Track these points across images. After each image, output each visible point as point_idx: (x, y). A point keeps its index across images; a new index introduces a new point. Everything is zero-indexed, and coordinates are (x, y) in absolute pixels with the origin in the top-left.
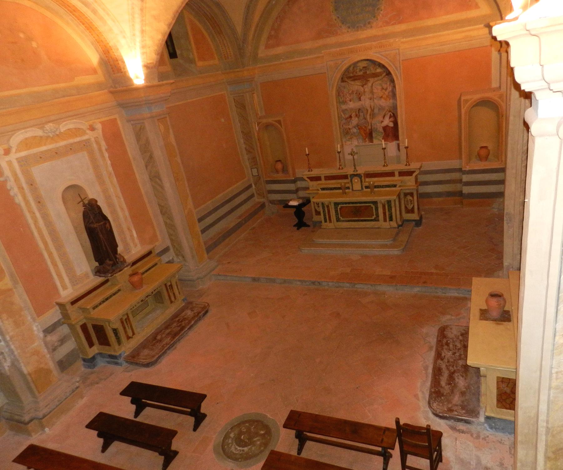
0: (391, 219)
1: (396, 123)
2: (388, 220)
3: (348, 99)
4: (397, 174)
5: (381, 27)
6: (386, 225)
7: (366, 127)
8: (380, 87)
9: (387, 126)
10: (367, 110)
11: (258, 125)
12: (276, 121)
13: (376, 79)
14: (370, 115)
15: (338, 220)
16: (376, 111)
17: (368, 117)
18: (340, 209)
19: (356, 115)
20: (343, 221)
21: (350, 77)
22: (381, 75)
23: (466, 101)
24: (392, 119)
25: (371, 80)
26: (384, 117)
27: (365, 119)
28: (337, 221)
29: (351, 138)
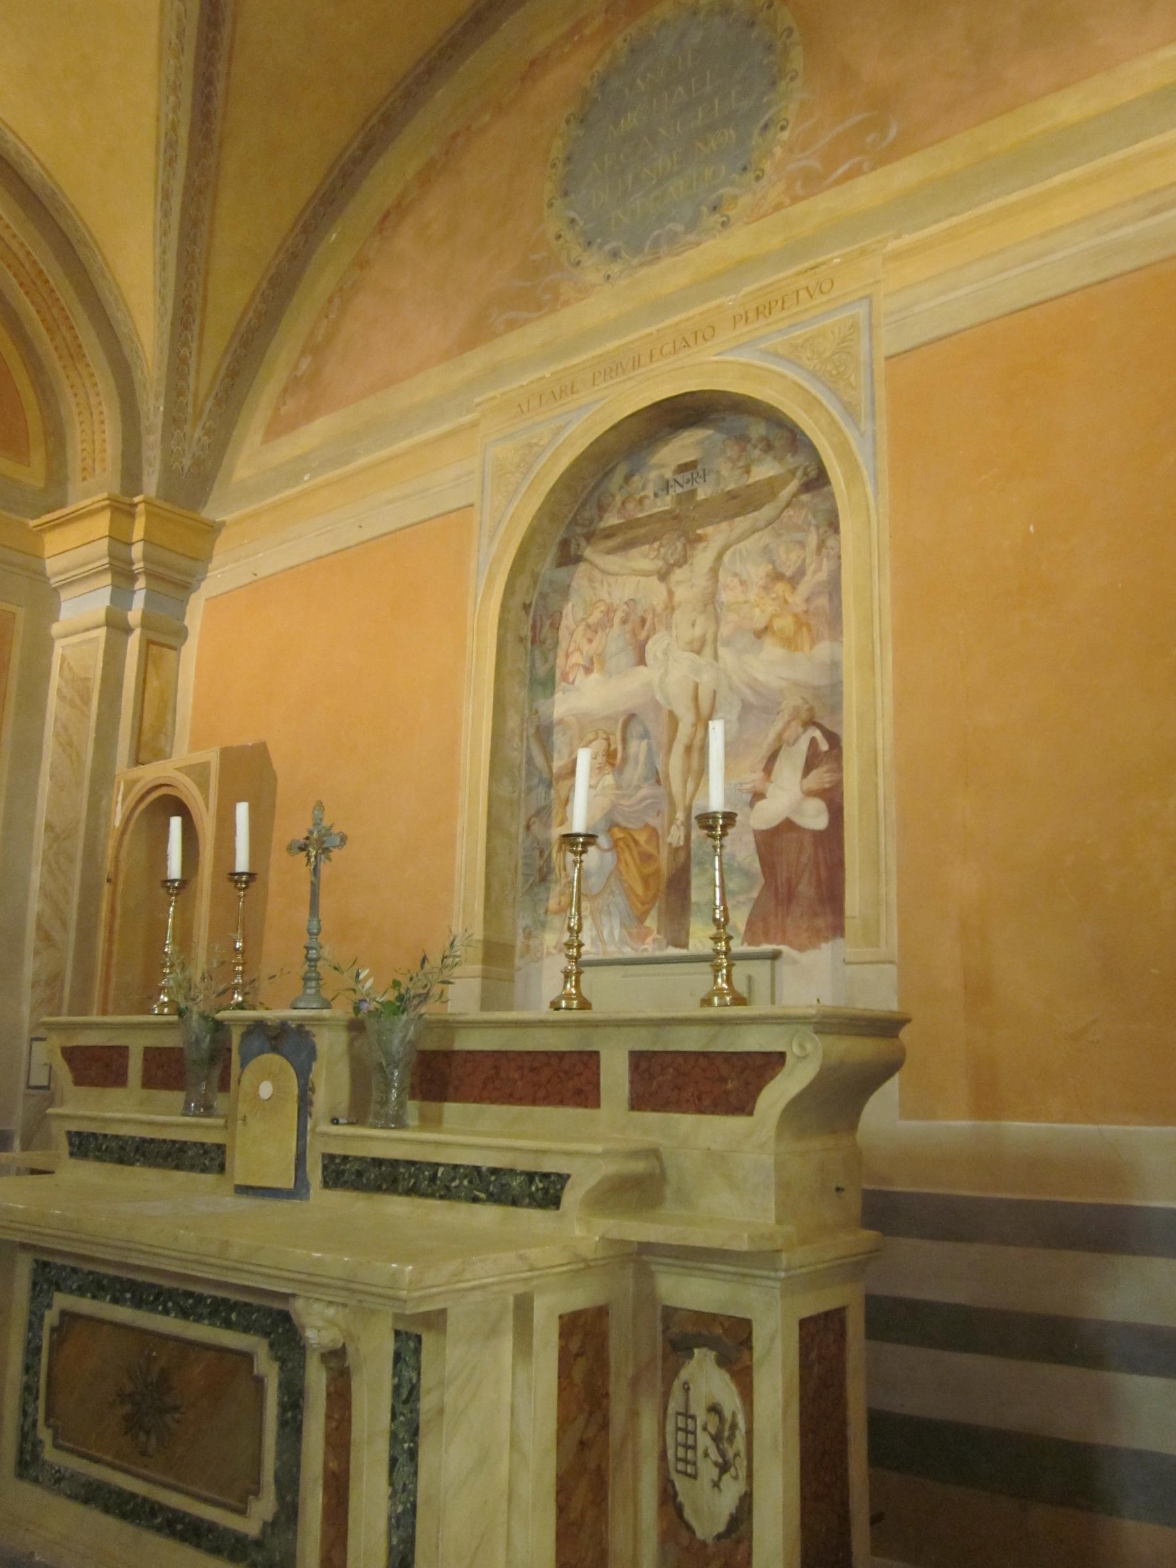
3: (576, 658)
4: (615, 1074)
5: (778, 207)
7: (654, 834)
9: (788, 826)
13: (742, 523)
20: (57, 1481)
22: (774, 495)
25: (717, 534)
26: (772, 758)
27: (657, 778)
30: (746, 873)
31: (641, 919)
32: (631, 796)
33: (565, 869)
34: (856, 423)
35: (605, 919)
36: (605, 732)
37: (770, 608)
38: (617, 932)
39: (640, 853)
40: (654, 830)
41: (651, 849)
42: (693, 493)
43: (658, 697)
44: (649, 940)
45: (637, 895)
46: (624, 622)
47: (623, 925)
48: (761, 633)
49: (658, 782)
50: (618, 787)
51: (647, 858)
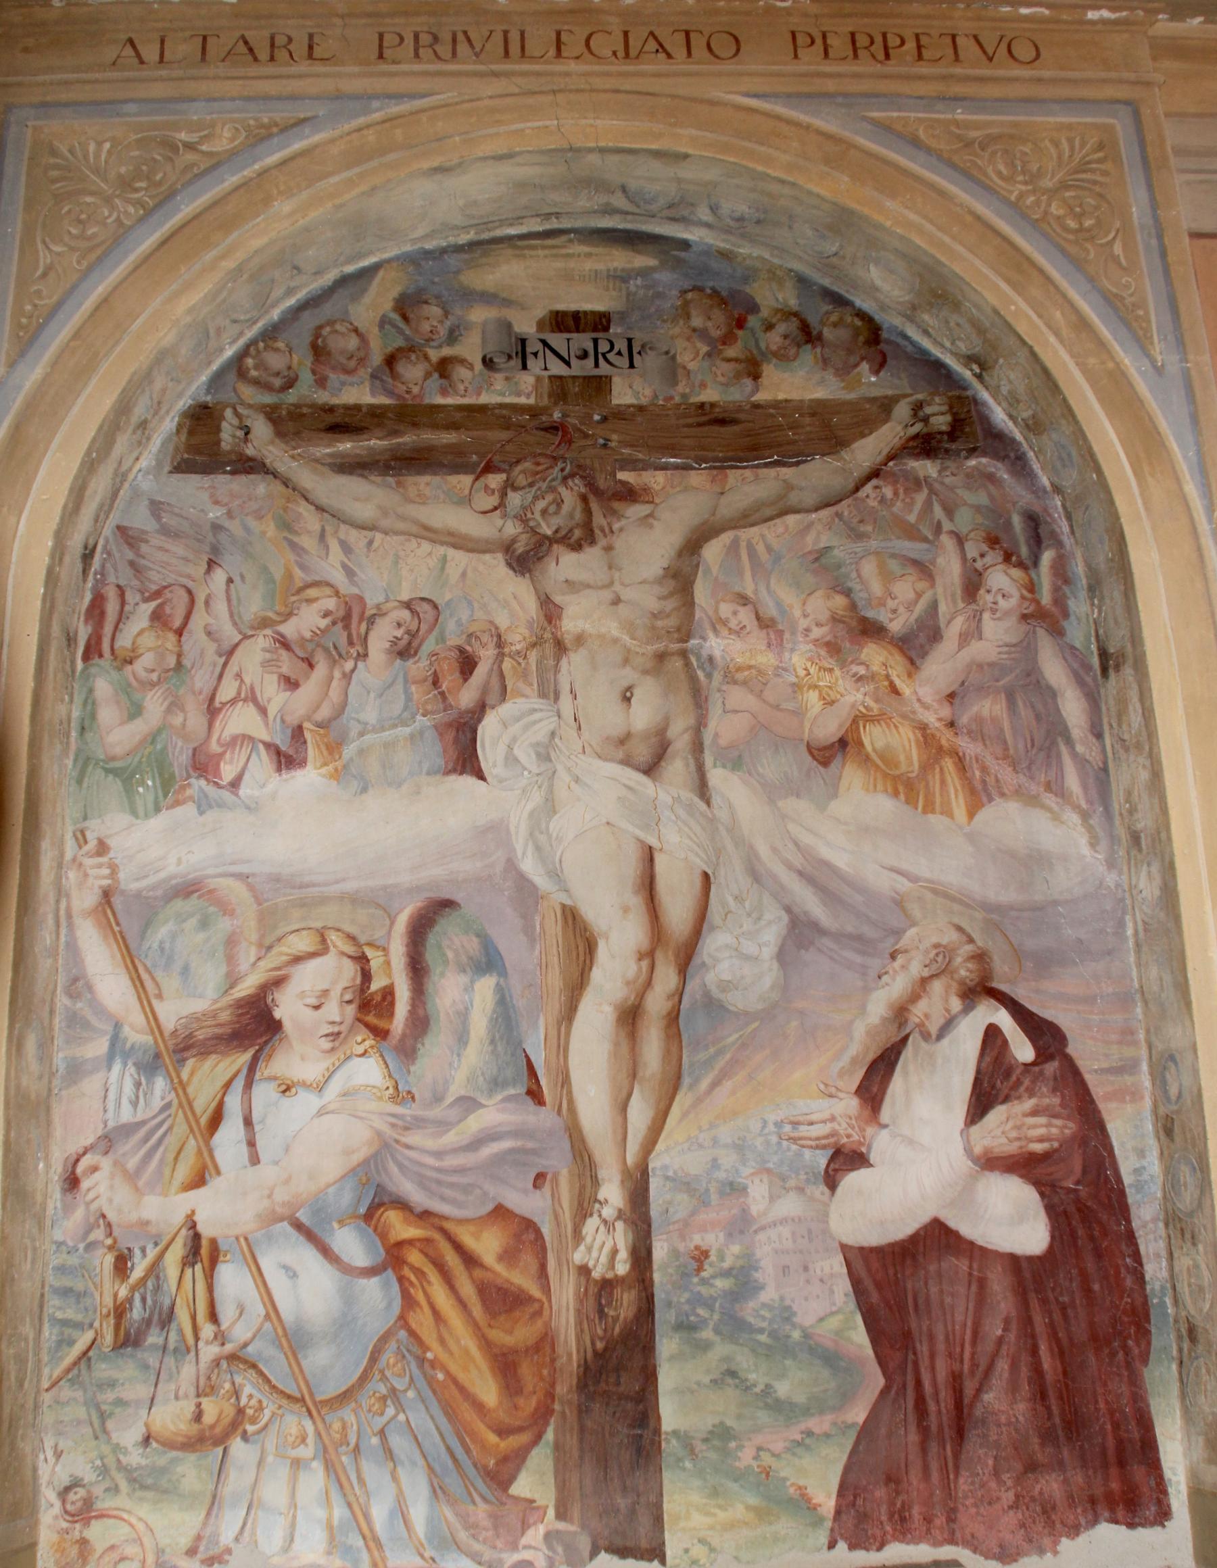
3: (241, 720)
7: (525, 1234)
8: (811, 610)
9: (937, 1238)
10: (581, 943)
13: (750, 485)
14: (630, 1017)
16: (742, 957)
19: (371, 1007)
21: (342, 423)
24: (1020, 1123)
25: (680, 498)
26: (880, 1069)
29: (208, 1439)
30: (833, 1359)
31: (500, 1476)
32: (443, 1126)
33: (213, 1317)
34: (1142, 343)
35: (374, 1472)
36: (352, 938)
37: (854, 697)
38: (419, 1513)
39: (483, 1290)
40: (529, 1225)
41: (521, 1279)
42: (598, 386)
43: (529, 865)
44: (535, 1535)
45: (479, 1407)
46: (404, 651)
47: (438, 1491)
48: (836, 751)
49: (535, 1094)
50: (401, 1096)
51: (503, 1301)
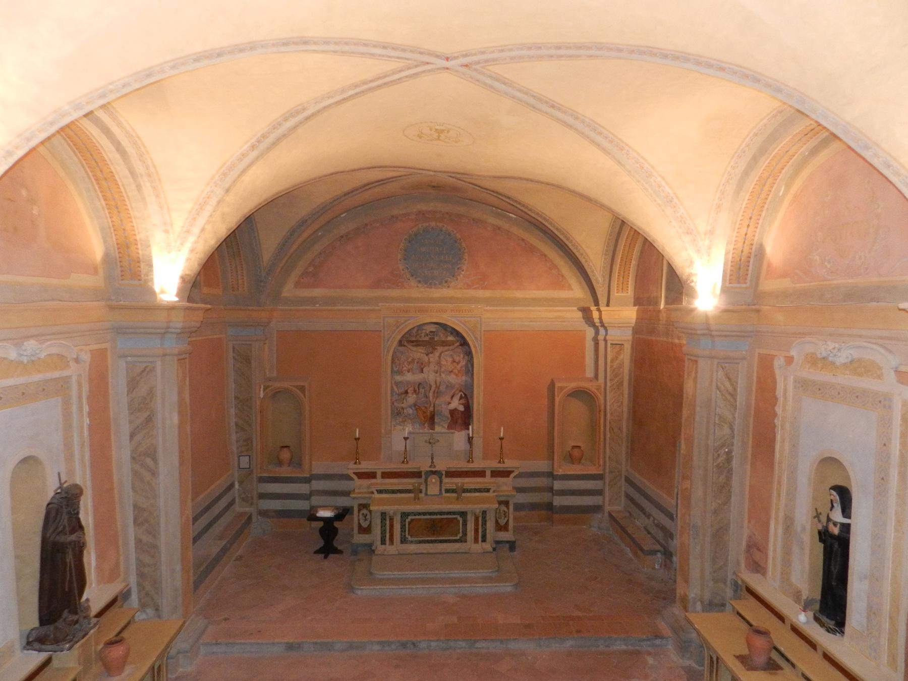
0: (484, 540)
1: (468, 408)
2: (480, 539)
4: (488, 473)
6: (478, 548)
8: (450, 360)
9: (456, 409)
11: (264, 390)
12: (297, 387)
13: (446, 348)
15: (403, 541)
16: (443, 388)
17: (431, 395)
18: (410, 523)
19: (415, 391)
20: (412, 542)
21: (413, 342)
23: (561, 388)
24: (463, 401)
25: (440, 349)
26: (452, 397)
27: (427, 397)
28: (402, 542)
29: (404, 422)
